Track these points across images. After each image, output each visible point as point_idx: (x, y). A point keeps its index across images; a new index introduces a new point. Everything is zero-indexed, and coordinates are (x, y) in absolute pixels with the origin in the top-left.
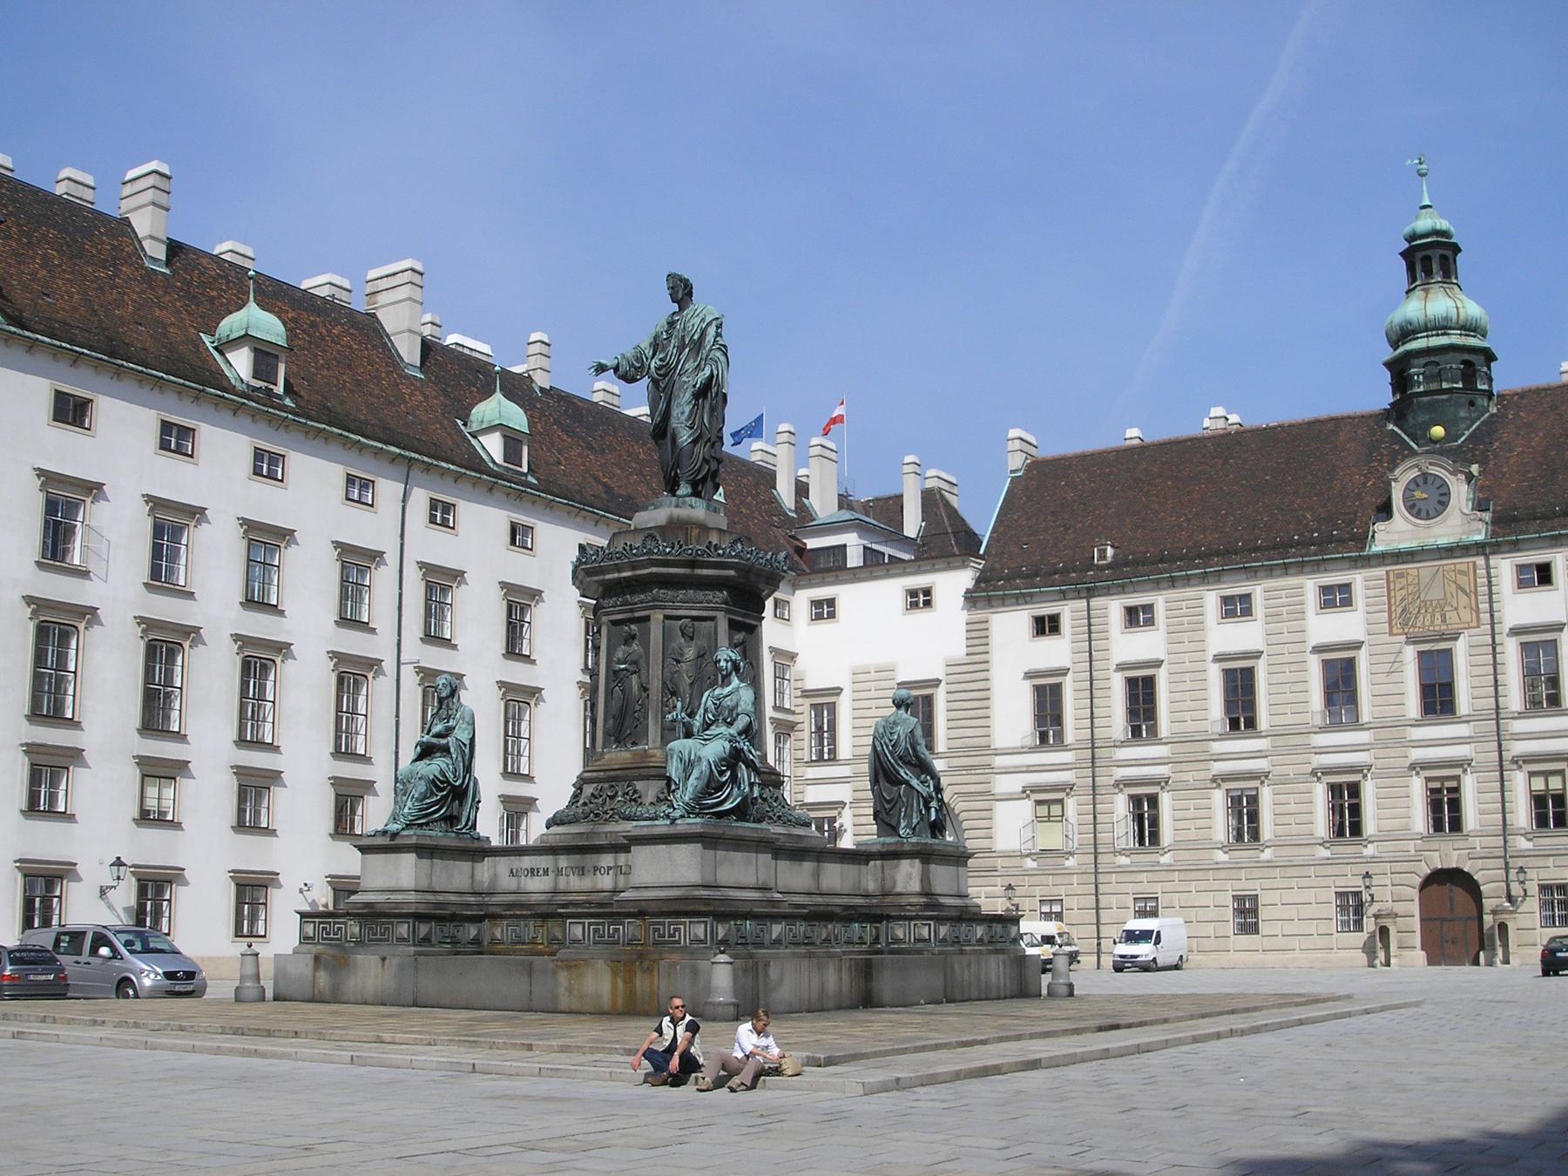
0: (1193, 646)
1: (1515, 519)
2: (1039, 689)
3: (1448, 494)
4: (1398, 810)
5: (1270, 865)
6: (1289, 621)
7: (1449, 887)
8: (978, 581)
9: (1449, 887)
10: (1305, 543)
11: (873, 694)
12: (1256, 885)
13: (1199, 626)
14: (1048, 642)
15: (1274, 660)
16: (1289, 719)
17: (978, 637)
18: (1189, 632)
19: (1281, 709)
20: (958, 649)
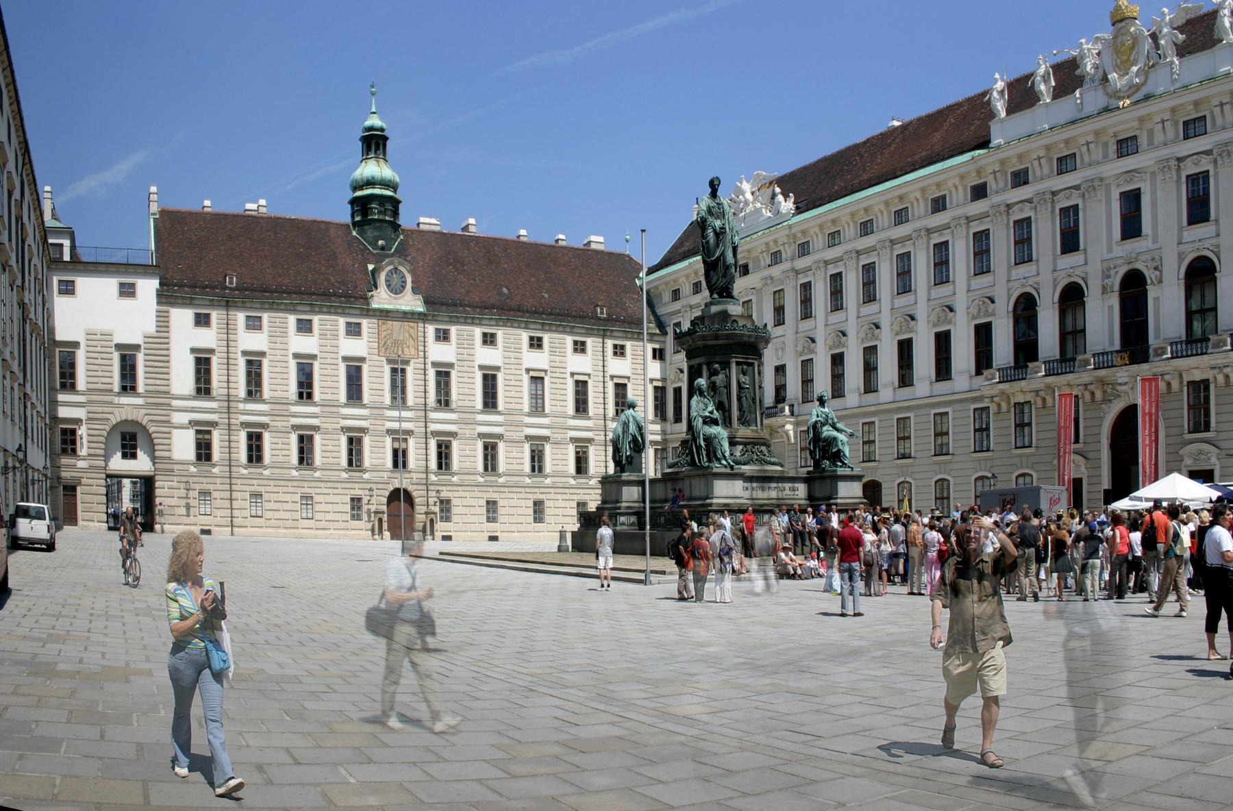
0: (282, 346)
1: (435, 303)
2: (199, 361)
3: (405, 282)
4: (377, 454)
5: (319, 480)
6: (331, 340)
7: (400, 498)
8: (161, 284)
9: (400, 498)
10: (334, 295)
11: (99, 349)
12: (309, 491)
13: (285, 334)
14: (202, 331)
15: (323, 361)
16: (329, 397)
17: (163, 323)
18: (280, 338)
19: (326, 390)
20: (151, 328)
